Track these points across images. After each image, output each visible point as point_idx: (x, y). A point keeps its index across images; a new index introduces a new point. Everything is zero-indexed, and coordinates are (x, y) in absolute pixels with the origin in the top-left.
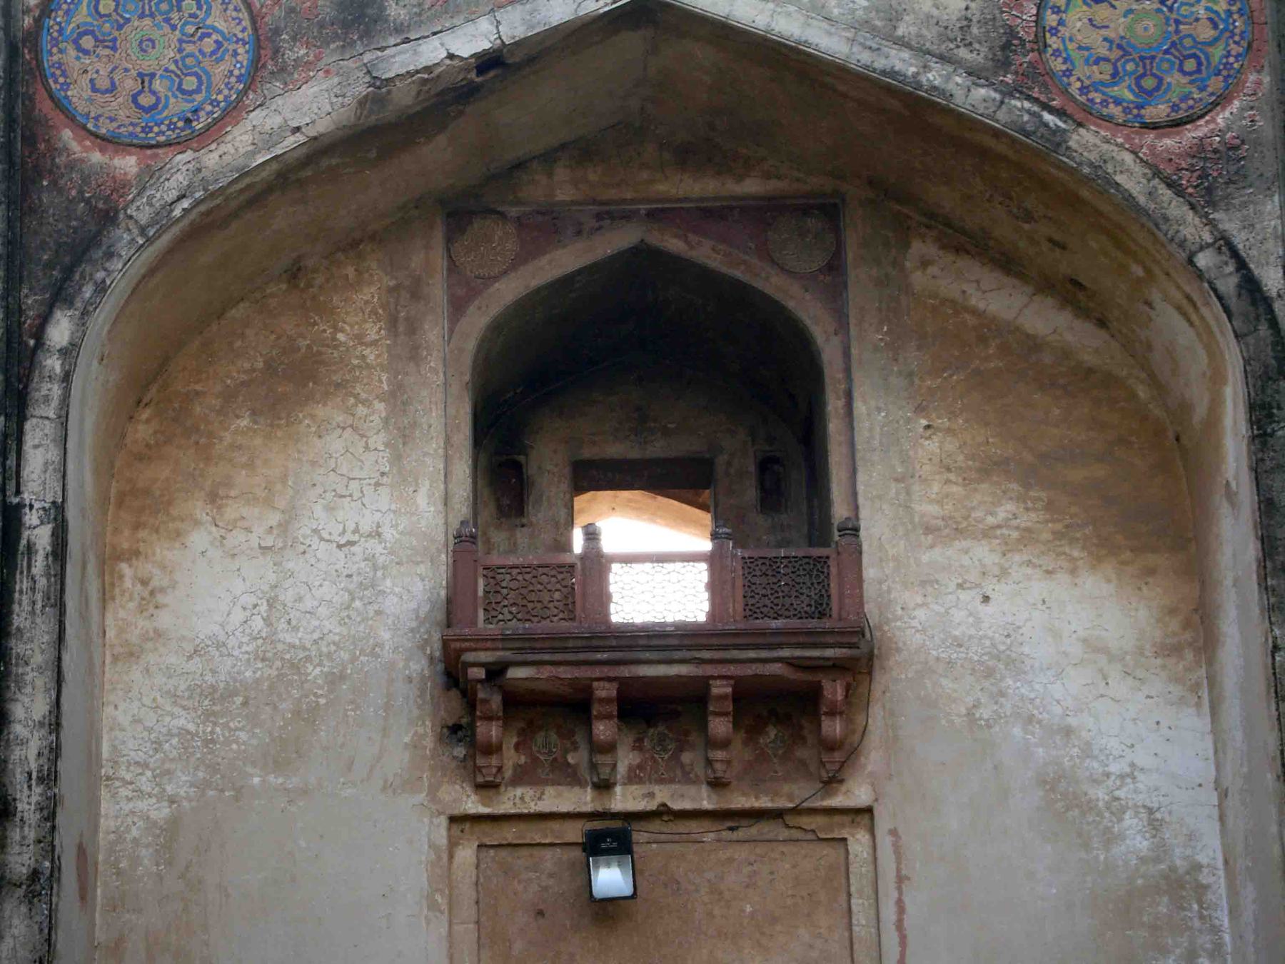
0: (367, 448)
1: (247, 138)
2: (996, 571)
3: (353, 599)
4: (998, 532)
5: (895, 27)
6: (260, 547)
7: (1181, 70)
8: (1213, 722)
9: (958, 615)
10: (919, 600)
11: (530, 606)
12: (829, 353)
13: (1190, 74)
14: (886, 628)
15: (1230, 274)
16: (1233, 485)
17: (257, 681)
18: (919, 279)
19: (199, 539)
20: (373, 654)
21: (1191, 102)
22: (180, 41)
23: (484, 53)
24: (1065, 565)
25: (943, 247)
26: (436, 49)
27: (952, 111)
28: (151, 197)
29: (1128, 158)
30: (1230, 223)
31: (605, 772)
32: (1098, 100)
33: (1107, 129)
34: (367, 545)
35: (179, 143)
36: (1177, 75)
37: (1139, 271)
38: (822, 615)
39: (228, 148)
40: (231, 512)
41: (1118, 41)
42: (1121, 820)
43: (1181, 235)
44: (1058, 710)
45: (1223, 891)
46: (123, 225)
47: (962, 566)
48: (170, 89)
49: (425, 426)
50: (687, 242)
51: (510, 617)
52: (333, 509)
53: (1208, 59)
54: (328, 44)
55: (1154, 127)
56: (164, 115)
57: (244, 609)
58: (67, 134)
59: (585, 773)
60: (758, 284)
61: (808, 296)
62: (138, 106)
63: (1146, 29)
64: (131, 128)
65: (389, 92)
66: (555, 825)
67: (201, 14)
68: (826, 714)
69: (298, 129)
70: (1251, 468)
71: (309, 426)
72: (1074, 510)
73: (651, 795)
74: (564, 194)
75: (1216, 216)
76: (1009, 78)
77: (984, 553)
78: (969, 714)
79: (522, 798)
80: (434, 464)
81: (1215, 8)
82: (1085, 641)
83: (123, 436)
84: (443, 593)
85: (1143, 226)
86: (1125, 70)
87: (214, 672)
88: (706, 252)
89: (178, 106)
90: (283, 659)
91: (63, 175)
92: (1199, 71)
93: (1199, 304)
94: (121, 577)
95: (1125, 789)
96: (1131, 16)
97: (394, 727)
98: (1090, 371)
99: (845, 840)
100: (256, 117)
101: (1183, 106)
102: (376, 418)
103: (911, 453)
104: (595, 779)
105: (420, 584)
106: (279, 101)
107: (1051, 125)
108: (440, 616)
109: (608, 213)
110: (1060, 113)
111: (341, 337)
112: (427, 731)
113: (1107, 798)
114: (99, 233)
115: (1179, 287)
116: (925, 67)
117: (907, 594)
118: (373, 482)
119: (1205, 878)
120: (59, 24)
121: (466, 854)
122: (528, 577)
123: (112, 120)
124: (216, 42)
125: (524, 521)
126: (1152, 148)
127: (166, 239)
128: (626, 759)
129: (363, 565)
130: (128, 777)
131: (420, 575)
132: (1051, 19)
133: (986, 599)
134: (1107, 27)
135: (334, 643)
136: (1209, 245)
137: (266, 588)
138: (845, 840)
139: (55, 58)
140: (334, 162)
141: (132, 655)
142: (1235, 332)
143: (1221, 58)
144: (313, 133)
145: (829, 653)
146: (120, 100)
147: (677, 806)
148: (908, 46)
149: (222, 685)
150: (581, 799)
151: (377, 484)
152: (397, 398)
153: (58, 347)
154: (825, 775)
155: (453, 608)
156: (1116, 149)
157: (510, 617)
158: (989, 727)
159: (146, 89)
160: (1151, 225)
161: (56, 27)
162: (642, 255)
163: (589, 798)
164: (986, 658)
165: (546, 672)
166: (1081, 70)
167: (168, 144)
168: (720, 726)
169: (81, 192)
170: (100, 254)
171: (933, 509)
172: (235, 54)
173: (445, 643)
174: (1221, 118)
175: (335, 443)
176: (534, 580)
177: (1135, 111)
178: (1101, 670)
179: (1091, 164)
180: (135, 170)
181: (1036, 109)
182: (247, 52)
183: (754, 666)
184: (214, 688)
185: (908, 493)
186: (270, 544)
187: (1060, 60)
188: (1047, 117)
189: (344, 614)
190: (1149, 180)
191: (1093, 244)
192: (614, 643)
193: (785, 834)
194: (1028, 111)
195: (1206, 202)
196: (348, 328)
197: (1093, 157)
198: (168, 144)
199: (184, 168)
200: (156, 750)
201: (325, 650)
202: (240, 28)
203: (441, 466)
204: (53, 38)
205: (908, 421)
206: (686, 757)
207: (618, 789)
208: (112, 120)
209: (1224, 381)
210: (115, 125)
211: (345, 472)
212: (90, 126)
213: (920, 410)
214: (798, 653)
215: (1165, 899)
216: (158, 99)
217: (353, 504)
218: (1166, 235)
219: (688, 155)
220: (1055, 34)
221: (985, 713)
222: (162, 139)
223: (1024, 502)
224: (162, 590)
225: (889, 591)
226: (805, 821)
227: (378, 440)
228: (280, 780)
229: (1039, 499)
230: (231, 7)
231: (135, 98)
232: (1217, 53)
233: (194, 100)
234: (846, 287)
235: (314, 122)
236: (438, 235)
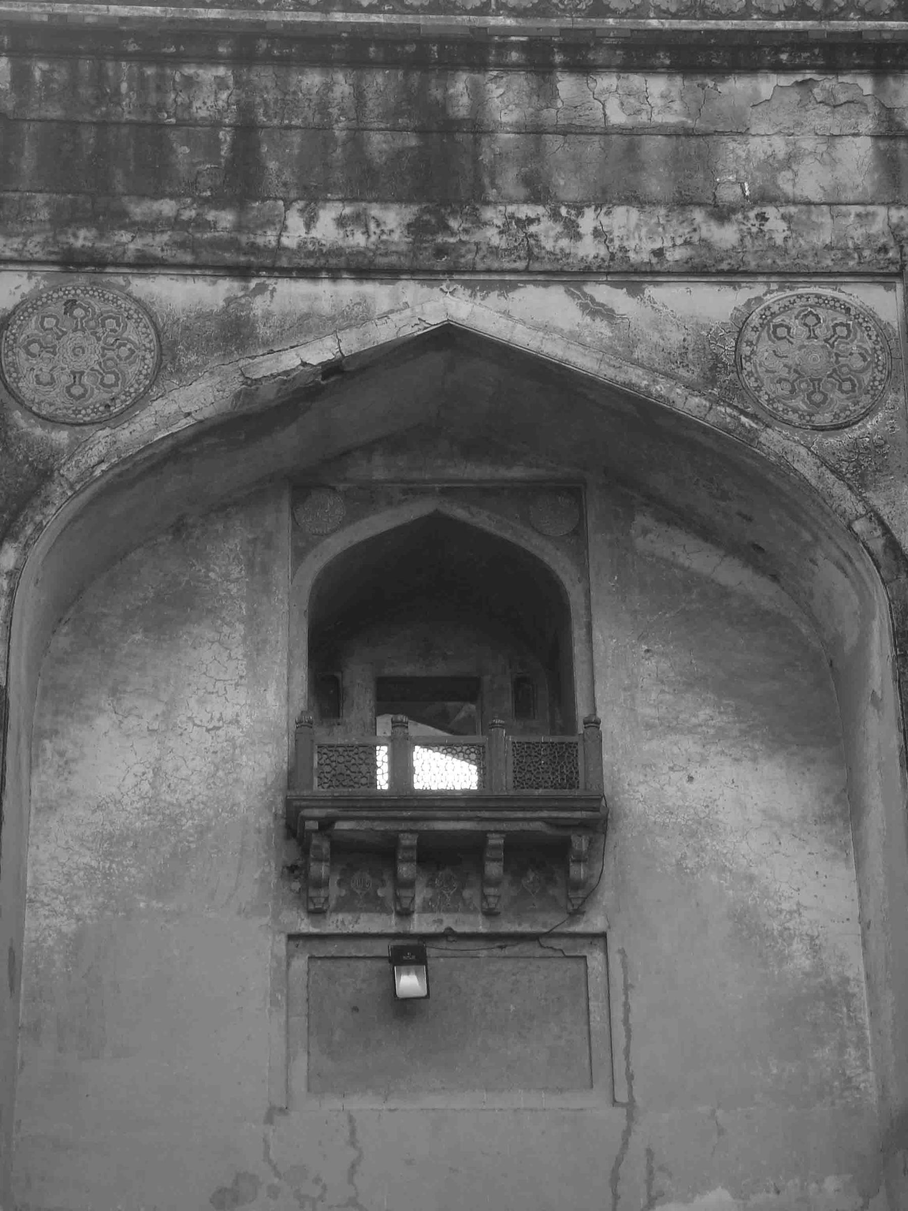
0: (230, 657)
1: (151, 420)
2: (698, 758)
3: (217, 770)
4: (699, 730)
5: (632, 353)
6: (149, 730)
7: (840, 389)
8: (857, 872)
9: (670, 790)
10: (642, 778)
11: (353, 775)
12: (575, 596)
13: (847, 392)
14: (616, 799)
15: (878, 537)
16: (879, 693)
17: (143, 830)
18: (640, 543)
19: (103, 723)
20: (232, 811)
21: (848, 413)
22: (103, 349)
23: (329, 362)
24: (749, 755)
25: (659, 520)
26: (293, 358)
27: (674, 413)
28: (78, 461)
29: (803, 451)
30: (877, 500)
31: (406, 903)
32: (781, 409)
33: (787, 429)
34: (230, 730)
35: (100, 422)
36: (838, 393)
37: (807, 536)
38: (572, 786)
39: (137, 427)
40: (128, 702)
41: (794, 367)
42: (790, 945)
43: (841, 508)
44: (744, 862)
45: (865, 997)
46: (57, 481)
47: (673, 754)
49: (273, 642)
50: (471, 513)
52: (204, 702)
53: (859, 382)
54: (212, 354)
55: (822, 429)
56: (90, 402)
57: (136, 776)
58: (17, 414)
59: (390, 904)
60: (523, 543)
61: (559, 554)
62: (71, 395)
63: (814, 360)
64: (65, 411)
65: (257, 388)
66: (368, 943)
67: (120, 330)
68: (573, 861)
69: (189, 414)
70: (895, 680)
71: (186, 640)
72: (754, 714)
73: (441, 921)
74: (379, 475)
75: (868, 494)
76: (716, 391)
77: (689, 745)
78: (679, 864)
79: (343, 922)
80: (279, 670)
81: (864, 346)
82: (764, 811)
83: (48, 646)
84: (285, 766)
85: (814, 501)
86: (799, 387)
87: (112, 823)
88: (484, 520)
89: (100, 396)
90: (164, 814)
91: (13, 444)
92: (853, 391)
93: (854, 561)
94: (44, 750)
95: (793, 922)
97: (247, 868)
98: (767, 613)
99: (585, 957)
100: (158, 405)
101: (842, 415)
102: (237, 635)
103: (636, 671)
104: (398, 908)
105: (268, 760)
106: (176, 393)
107: (747, 425)
108: (283, 783)
109: (411, 489)
110: (753, 417)
111: (212, 575)
112: (272, 871)
113: (780, 928)
114: (39, 487)
115: (838, 547)
116: (654, 381)
117: (632, 773)
118: (233, 682)
119: (852, 988)
120: (14, 334)
121: (300, 963)
122: (351, 754)
123: (51, 405)
124: (130, 349)
125: (340, 720)
126: (820, 444)
127: (88, 493)
128: (421, 894)
129: (225, 744)
130: (46, 900)
131: (268, 753)
132: (746, 350)
133: (691, 779)
134: (786, 357)
135: (202, 803)
136: (862, 516)
137: (152, 760)
138: (585, 957)
139: (10, 359)
140: (213, 440)
141: (51, 808)
142: (882, 579)
143: (869, 384)
144: (200, 417)
145: (578, 814)
146: (58, 390)
147: (459, 929)
148: (642, 366)
149: (117, 832)
150: (387, 923)
151: (237, 685)
152: (253, 621)
153: (5, 571)
154: (570, 908)
155: (293, 776)
156: (794, 444)
158: (693, 874)
159: (77, 382)
160: (820, 500)
161: (12, 337)
162: (436, 520)
163: (393, 922)
164: (690, 822)
165: (365, 825)
166: (768, 387)
167: (92, 423)
168: (494, 869)
169: (26, 457)
170: (39, 502)
171: (649, 711)
172: (144, 359)
173: (288, 802)
174: (870, 425)
175: (206, 653)
176: (356, 757)
177: (808, 418)
178: (775, 833)
179: (776, 455)
180: (66, 441)
181: (735, 413)
182: (152, 358)
183: (521, 824)
184: (111, 836)
185: (633, 699)
186: (156, 727)
187: (753, 379)
188: (744, 419)
189: (210, 781)
190: (818, 468)
191: (774, 517)
192: (416, 804)
193: (539, 952)
194: (730, 415)
195: (860, 484)
196: (217, 569)
197: (778, 449)
198: (92, 423)
199: (103, 441)
200: (68, 881)
201: (195, 807)
202: (147, 340)
203: (285, 672)
204: (9, 345)
205: (633, 646)
206: (467, 893)
207: (415, 916)
208: (51, 405)
209: (873, 618)
210: (53, 408)
211: (212, 673)
212: (34, 409)
213: (642, 638)
214: (555, 814)
215: (823, 1004)
216: (86, 391)
217: (219, 700)
218: (831, 507)
219: (473, 449)
220: (749, 361)
221: (690, 863)
222: (87, 419)
223: (719, 708)
224: (74, 760)
225: (619, 771)
226: (554, 943)
227: (238, 652)
228: (160, 905)
229: (729, 705)
230: (141, 325)
231: (68, 389)
232: (866, 378)
233: (112, 392)
234: (587, 547)
235: (201, 409)
236: (286, 505)
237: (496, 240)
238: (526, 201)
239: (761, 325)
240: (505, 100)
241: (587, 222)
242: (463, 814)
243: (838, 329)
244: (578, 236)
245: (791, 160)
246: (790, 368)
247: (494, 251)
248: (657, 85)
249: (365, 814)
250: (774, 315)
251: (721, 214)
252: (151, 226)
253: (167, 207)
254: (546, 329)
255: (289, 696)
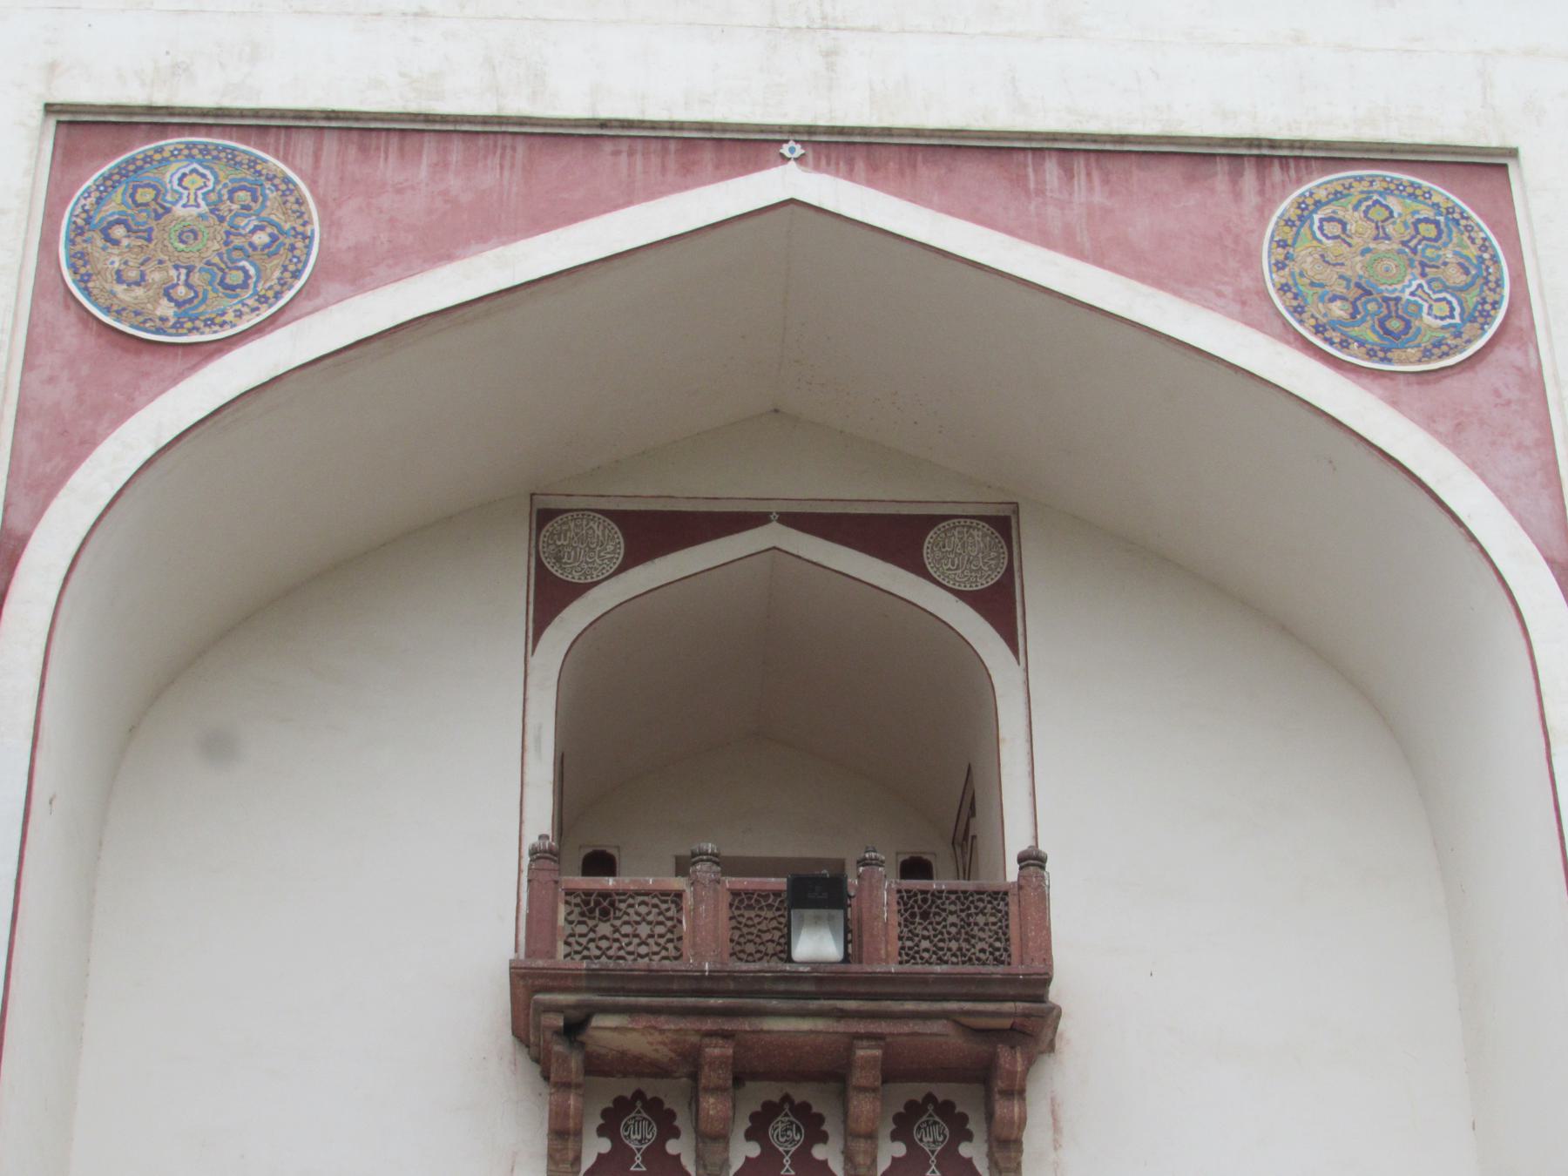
22: (228, 233)
48: (210, 283)
51: (598, 953)
53: (1461, 304)
81: (1465, 252)
96: (1368, 256)
143: (1475, 309)
145: (1008, 1006)
157: (598, 953)
172: (293, 248)
208: (137, 314)
210: (141, 319)
216: (196, 296)
239: (1300, 218)
242: (814, 1005)
243: (1422, 227)
246: (1348, 280)
249: (643, 1000)
250: (1318, 204)
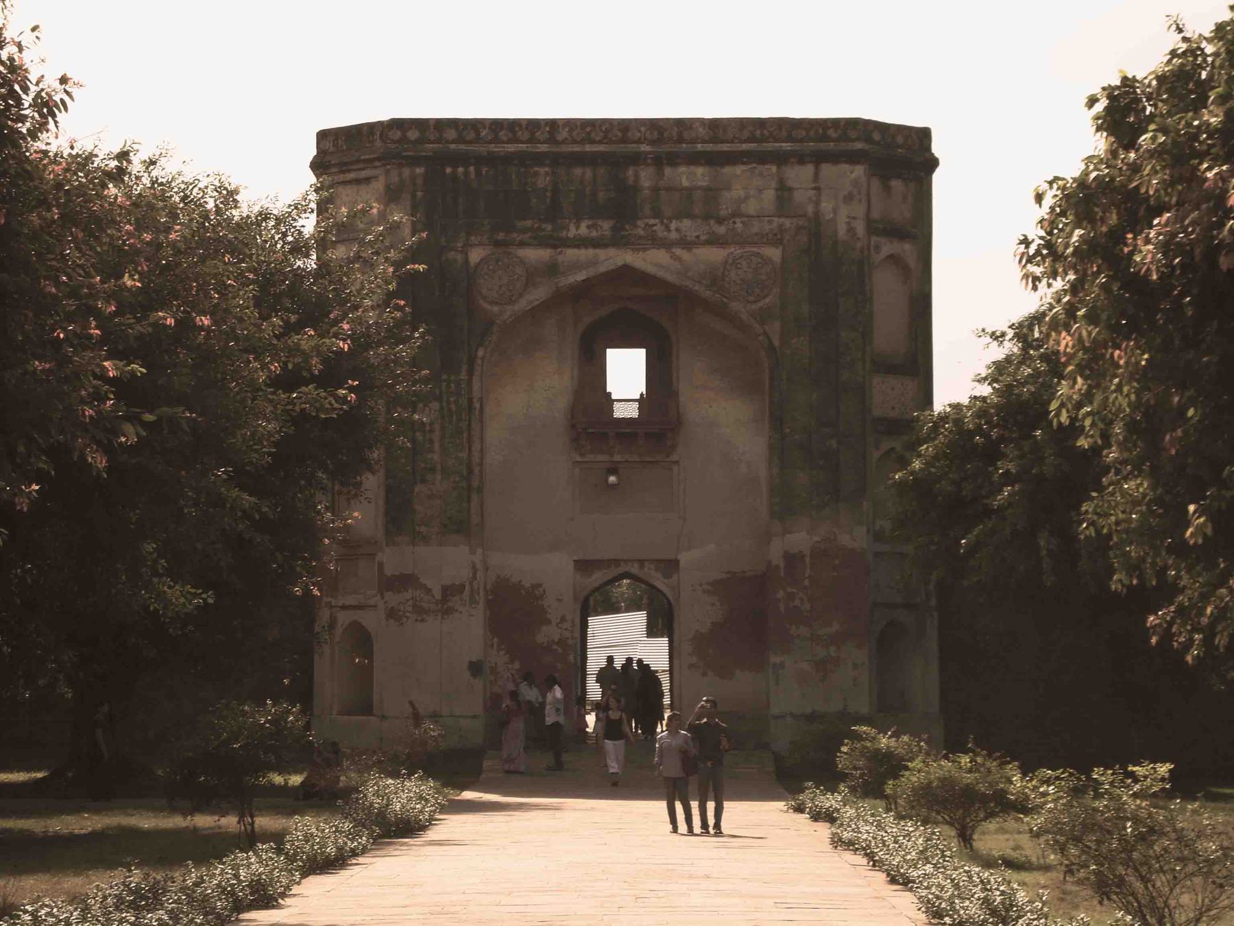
121: (577, 470)
174: (767, 300)
237: (642, 233)
238: (654, 218)
240: (646, 177)
241: (673, 225)
244: (669, 231)
245: (747, 198)
247: (641, 237)
248: (700, 170)
251: (720, 221)
252: (524, 231)
253: (529, 223)
254: (660, 266)
255: (573, 377)
